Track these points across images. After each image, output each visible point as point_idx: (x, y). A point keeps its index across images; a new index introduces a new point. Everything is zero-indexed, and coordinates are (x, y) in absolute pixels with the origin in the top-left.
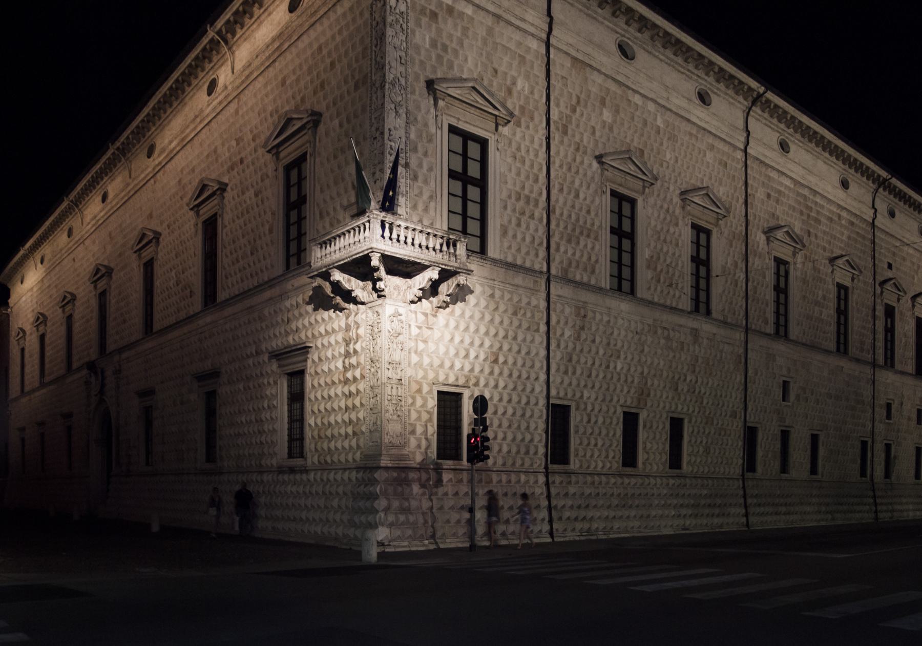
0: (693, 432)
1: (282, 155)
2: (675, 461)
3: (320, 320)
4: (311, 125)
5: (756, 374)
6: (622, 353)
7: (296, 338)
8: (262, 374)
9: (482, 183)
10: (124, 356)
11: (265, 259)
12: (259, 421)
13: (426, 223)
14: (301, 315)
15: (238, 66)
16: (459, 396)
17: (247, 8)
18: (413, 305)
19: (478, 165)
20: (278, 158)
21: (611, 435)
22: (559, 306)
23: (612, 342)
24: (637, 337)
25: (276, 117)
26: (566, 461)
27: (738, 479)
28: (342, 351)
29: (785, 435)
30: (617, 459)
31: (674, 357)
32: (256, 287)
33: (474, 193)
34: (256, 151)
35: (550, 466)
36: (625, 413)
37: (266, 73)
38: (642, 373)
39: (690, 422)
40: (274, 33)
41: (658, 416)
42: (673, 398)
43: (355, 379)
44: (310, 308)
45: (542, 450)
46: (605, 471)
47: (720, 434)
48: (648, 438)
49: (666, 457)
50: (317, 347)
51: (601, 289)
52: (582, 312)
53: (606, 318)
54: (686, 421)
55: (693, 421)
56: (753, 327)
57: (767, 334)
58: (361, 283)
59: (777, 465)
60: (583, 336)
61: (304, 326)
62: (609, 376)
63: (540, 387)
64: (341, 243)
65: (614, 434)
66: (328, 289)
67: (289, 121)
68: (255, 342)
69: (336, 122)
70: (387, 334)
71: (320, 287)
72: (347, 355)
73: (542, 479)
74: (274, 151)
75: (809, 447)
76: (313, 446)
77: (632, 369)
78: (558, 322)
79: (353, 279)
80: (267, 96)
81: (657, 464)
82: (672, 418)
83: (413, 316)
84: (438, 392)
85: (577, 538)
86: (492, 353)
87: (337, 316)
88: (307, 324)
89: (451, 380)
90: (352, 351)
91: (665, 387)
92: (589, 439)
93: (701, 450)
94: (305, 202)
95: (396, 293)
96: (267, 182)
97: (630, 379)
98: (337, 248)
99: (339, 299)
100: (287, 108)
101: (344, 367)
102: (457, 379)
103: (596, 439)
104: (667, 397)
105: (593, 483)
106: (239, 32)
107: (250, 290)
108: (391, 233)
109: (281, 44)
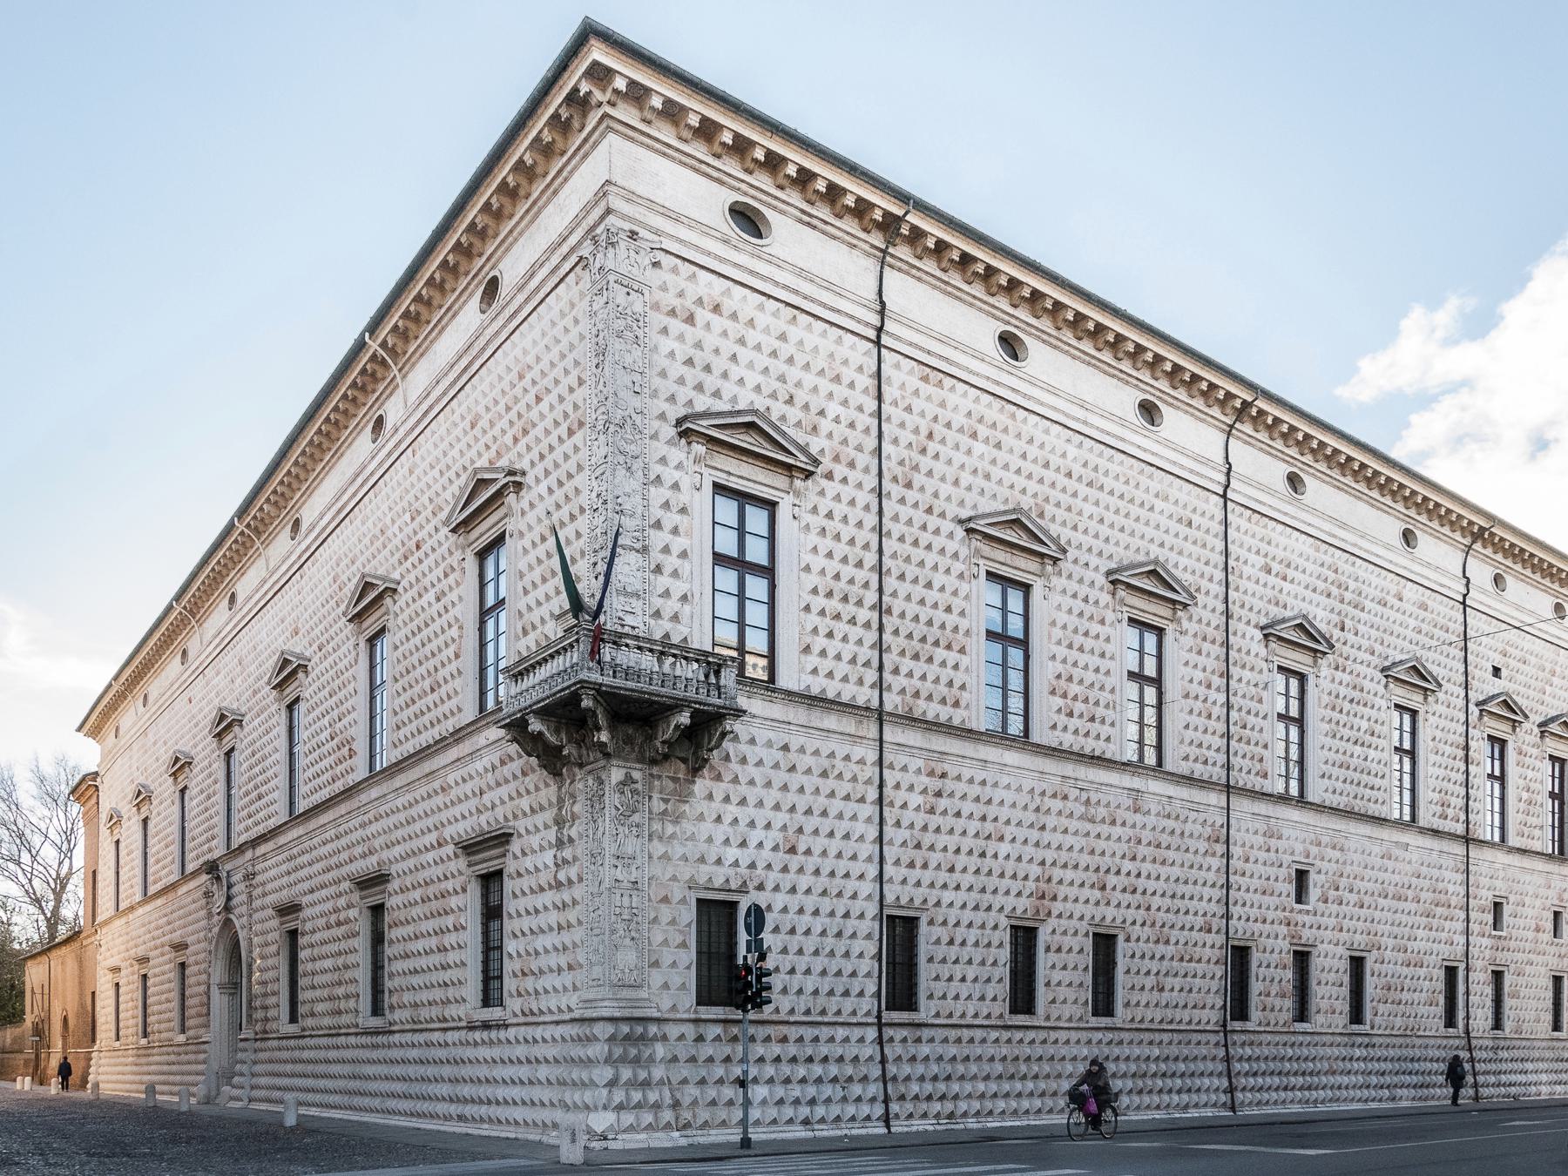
2: (1103, 1003)
9: (768, 572)
16: (733, 905)
19: (764, 544)
25: (464, 477)
26: (911, 1006)
29: (1302, 959)
33: (756, 587)
35: (885, 1014)
43: (570, 882)
45: (871, 988)
54: (1121, 939)
63: (868, 887)
70: (614, 811)
72: (560, 844)
73: (872, 1033)
75: (1346, 979)
78: (897, 786)
84: (699, 900)
86: (785, 838)
89: (718, 882)
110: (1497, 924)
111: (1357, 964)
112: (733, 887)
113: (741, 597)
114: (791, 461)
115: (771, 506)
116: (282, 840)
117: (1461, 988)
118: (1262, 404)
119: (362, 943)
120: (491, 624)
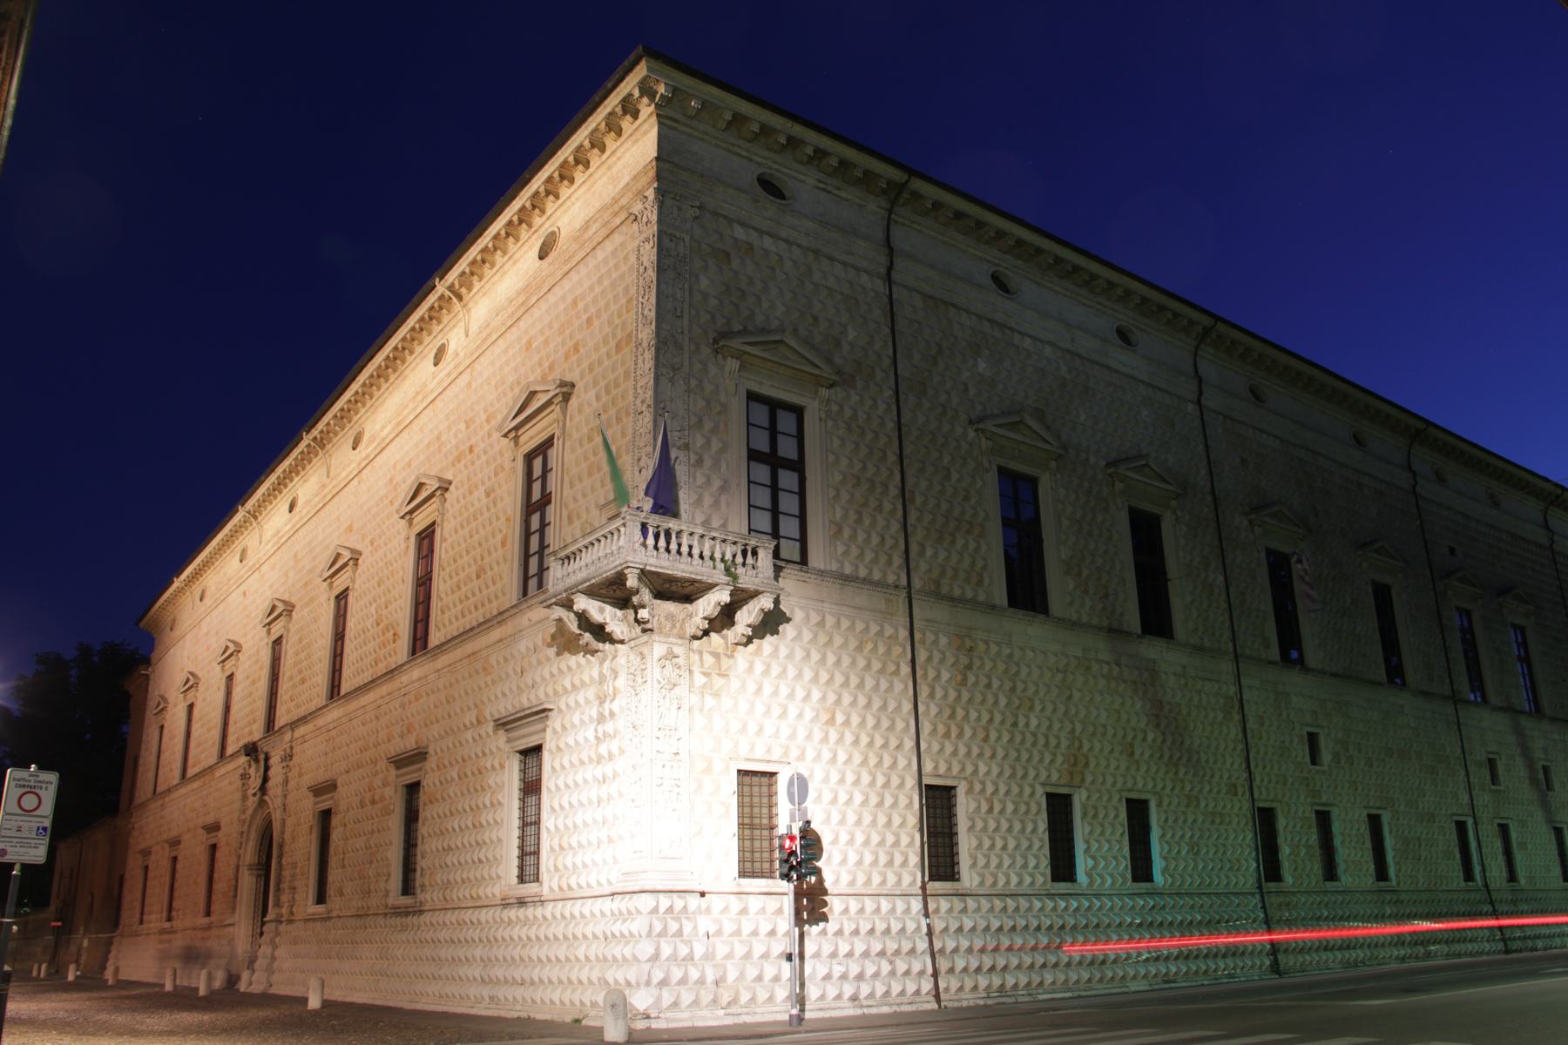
0: (1166, 820)
1: (522, 440)
3: (565, 669)
4: (560, 398)
5: (1262, 724)
6: (1037, 702)
7: (532, 697)
8: (484, 754)
10: (301, 730)
11: (494, 583)
12: (477, 826)
13: (716, 523)
14: (539, 662)
15: (474, 328)
17: (487, 257)
18: (696, 643)
20: (516, 444)
21: (1029, 830)
22: (930, 637)
23: (1020, 686)
24: (1060, 676)
25: (517, 390)
27: (1253, 894)
28: (594, 713)
30: (1042, 869)
31: (1123, 704)
32: (480, 625)
34: (489, 435)
36: (1049, 796)
37: (507, 335)
38: (1073, 731)
39: (1159, 805)
40: (520, 285)
41: (1105, 798)
42: (1128, 769)
44: (552, 651)
46: (1024, 889)
47: (1213, 822)
48: (1091, 832)
49: (1125, 863)
50: (560, 710)
51: (994, 607)
52: (968, 643)
53: (1007, 651)
55: (1165, 803)
56: (1247, 652)
57: (1270, 663)
58: (619, 613)
59: (1317, 868)
60: (971, 679)
61: (543, 679)
62: (1018, 739)
64: (587, 557)
65: (1034, 830)
66: (573, 626)
67: (533, 394)
68: (476, 706)
69: (592, 393)
71: (560, 620)
74: (513, 434)
76: (551, 863)
77: (1056, 726)
79: (608, 608)
80: (507, 363)
81: (1112, 876)
82: (1129, 801)
83: (697, 657)
85: (982, 1002)
87: (589, 662)
88: (547, 676)
90: (607, 713)
91: (1112, 751)
92: (992, 839)
93: (1185, 849)
94: (549, 502)
95: (669, 625)
96: (502, 475)
97: (1053, 742)
98: (583, 563)
99: (587, 636)
100: (531, 379)
101: (597, 738)
102: (769, 751)
103: (1004, 839)
104: (1118, 768)
105: (1005, 909)
106: (477, 286)
107: (472, 629)
108: (668, 543)
109: (528, 298)
110: (1494, 779)
111: (1375, 822)
112: (775, 757)
113: (775, 489)
114: (817, 372)
115: (798, 411)
116: (321, 721)
117: (1473, 845)
118: (1221, 327)
119: (395, 824)
120: (535, 518)
